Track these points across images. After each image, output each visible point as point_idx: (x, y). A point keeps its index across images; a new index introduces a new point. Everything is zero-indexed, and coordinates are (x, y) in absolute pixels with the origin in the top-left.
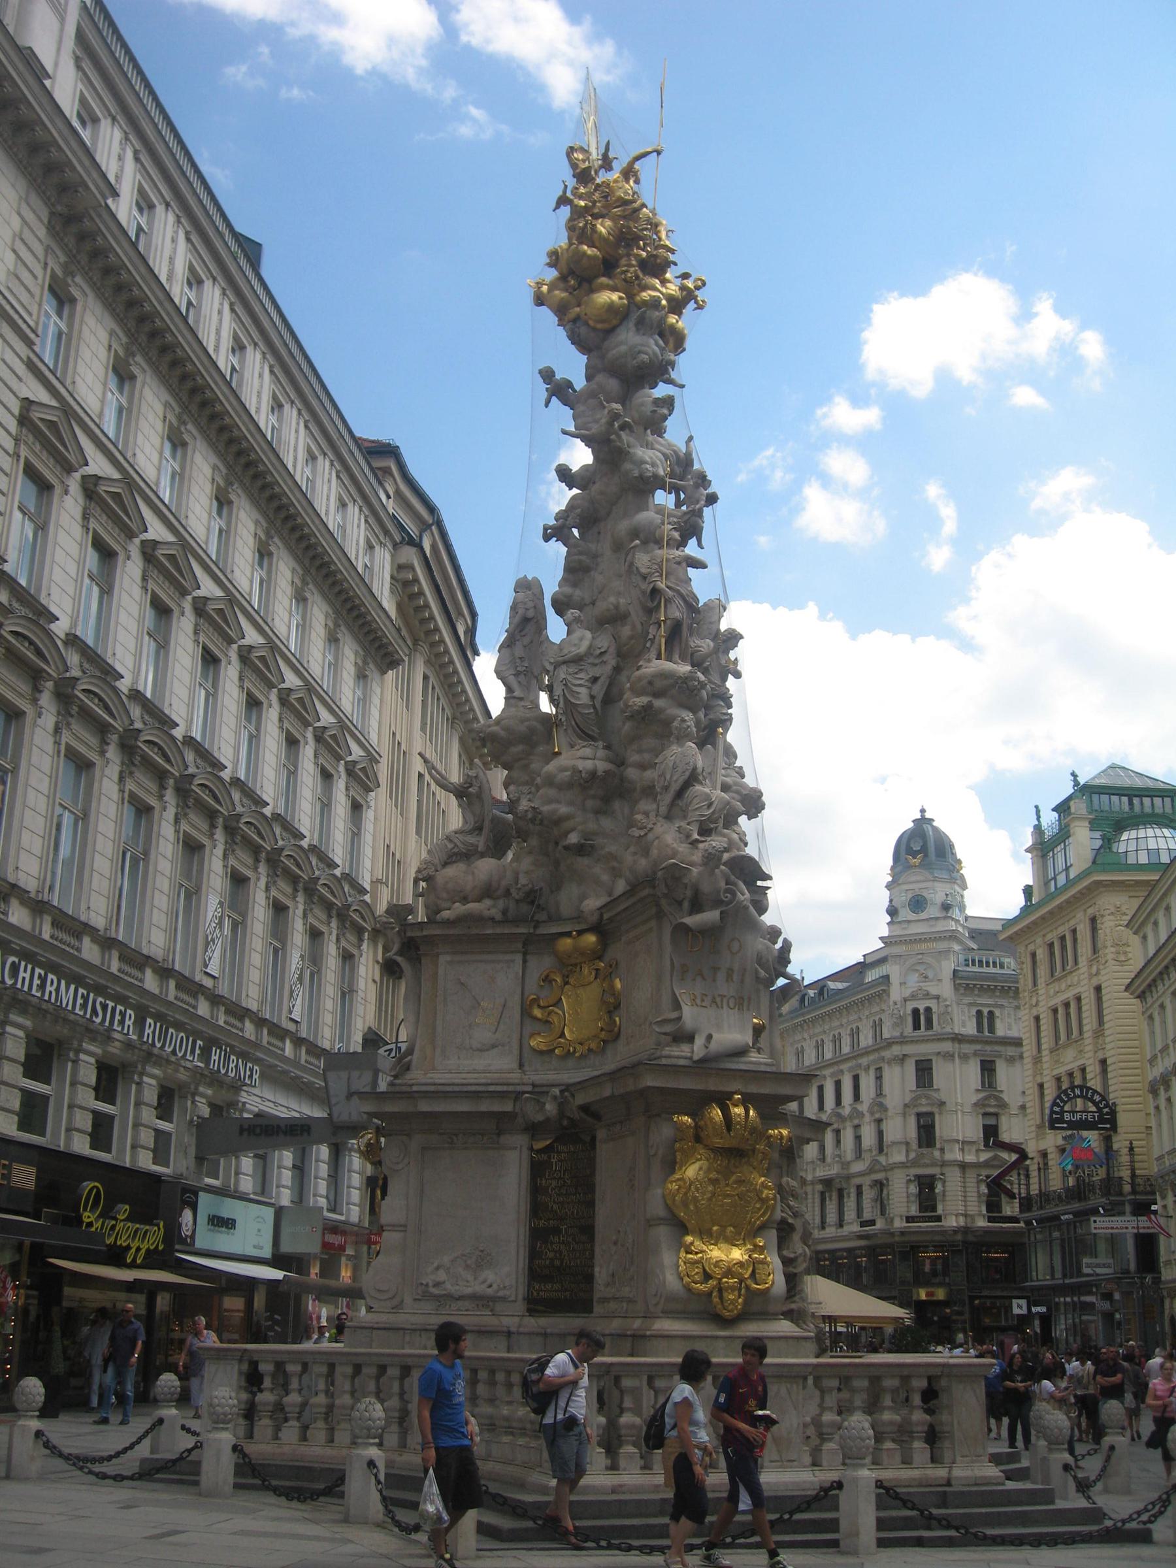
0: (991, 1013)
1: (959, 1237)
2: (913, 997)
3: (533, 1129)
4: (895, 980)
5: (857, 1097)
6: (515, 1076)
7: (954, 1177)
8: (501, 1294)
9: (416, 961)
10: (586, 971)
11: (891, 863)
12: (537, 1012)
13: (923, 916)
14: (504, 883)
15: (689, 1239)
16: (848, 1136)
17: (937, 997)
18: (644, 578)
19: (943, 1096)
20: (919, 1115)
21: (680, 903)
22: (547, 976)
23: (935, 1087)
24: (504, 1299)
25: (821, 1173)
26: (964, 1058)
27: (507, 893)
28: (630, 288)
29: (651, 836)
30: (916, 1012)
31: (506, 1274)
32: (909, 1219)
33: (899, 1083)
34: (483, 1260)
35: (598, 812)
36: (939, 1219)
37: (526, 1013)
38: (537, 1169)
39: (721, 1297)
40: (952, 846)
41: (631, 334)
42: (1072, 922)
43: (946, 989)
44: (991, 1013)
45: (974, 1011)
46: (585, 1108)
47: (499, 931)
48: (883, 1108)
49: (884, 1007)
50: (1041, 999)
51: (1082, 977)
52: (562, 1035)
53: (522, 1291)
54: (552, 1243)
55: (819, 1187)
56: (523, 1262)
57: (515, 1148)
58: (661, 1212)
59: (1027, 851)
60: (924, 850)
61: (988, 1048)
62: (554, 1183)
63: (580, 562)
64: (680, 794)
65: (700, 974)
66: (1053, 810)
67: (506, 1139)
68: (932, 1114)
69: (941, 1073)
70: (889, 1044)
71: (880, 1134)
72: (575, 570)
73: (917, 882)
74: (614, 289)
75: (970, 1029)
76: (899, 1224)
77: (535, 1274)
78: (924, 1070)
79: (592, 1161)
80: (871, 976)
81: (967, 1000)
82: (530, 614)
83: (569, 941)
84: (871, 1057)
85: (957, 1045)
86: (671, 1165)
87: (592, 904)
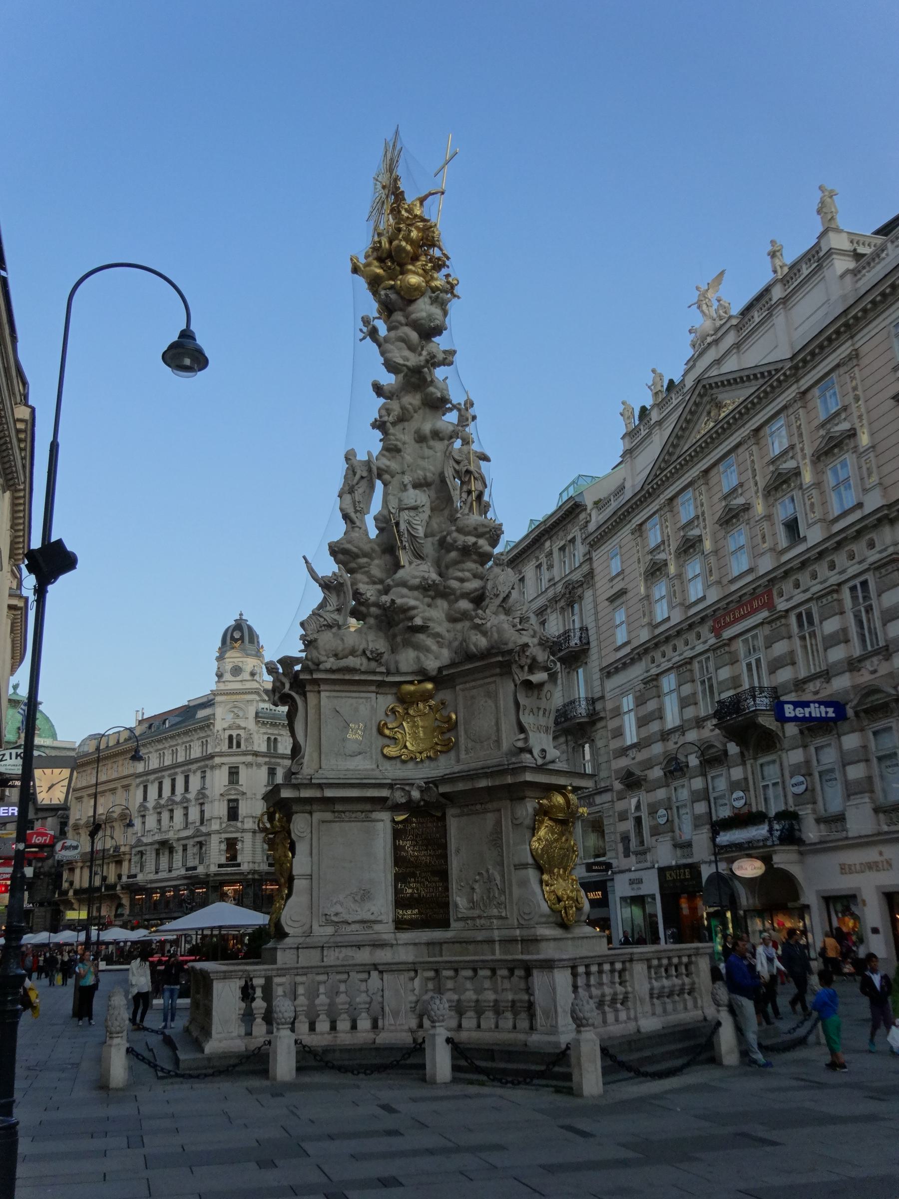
0: (275, 739)
1: (250, 876)
2: (230, 728)
3: (396, 808)
4: (218, 716)
5: (187, 789)
6: (377, 773)
7: (248, 837)
8: (379, 919)
9: (304, 695)
10: (421, 705)
11: (219, 645)
12: (387, 732)
14: (362, 647)
15: (546, 877)
16: (178, 814)
17: (245, 729)
18: (458, 462)
19: (243, 789)
20: (229, 801)
21: (522, 667)
22: (392, 708)
24: (380, 922)
25: (157, 837)
26: (259, 765)
27: (364, 652)
29: (489, 624)
30: (231, 737)
31: (382, 905)
32: (220, 866)
33: (219, 780)
34: (365, 896)
35: (429, 606)
36: (239, 865)
37: (380, 732)
38: (397, 834)
39: (566, 913)
40: (258, 637)
41: (428, 307)
43: (250, 724)
44: (275, 739)
45: (266, 737)
46: (443, 795)
47: (363, 677)
48: (205, 796)
49: (209, 733)
52: (405, 747)
53: (391, 917)
54: (409, 883)
55: (157, 846)
56: (390, 896)
57: (383, 821)
58: (530, 860)
60: (242, 638)
61: (273, 760)
62: (408, 843)
63: (396, 446)
64: (505, 599)
65: (532, 711)
67: (376, 815)
68: (237, 801)
69: (244, 774)
70: (211, 757)
71: (202, 812)
72: (391, 449)
73: (234, 657)
75: (263, 748)
76: (213, 869)
77: (400, 903)
78: (234, 773)
79: (444, 830)
80: (201, 714)
81: (263, 730)
82: (365, 474)
83: (411, 688)
84: (199, 764)
86: (534, 830)
87: (432, 665)
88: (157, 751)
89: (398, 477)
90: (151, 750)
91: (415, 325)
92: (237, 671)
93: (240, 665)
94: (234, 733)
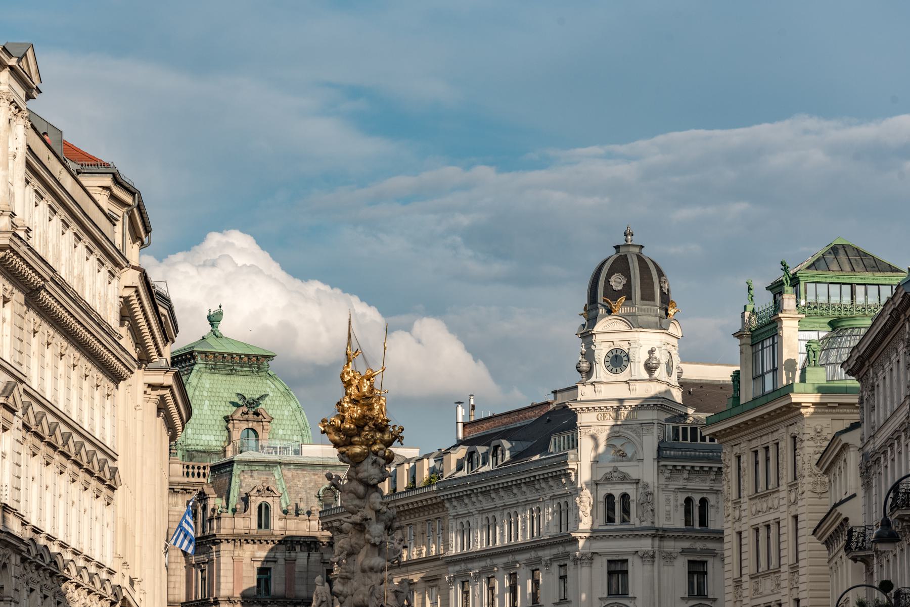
0: (703, 501)
2: (608, 480)
11: (584, 300)
13: (623, 376)
17: (637, 482)
23: (630, 595)
26: (669, 557)
28: (369, 444)
42: (776, 436)
43: (647, 471)
44: (703, 501)
45: (685, 496)
50: (743, 514)
51: (782, 502)
59: (739, 335)
60: (627, 292)
66: (767, 288)
74: (361, 444)
75: (678, 521)
85: (657, 542)
88: (482, 512)
89: (350, 597)
90: (471, 508)
91: (361, 481)
92: (618, 360)
93: (625, 347)
94: (617, 491)
